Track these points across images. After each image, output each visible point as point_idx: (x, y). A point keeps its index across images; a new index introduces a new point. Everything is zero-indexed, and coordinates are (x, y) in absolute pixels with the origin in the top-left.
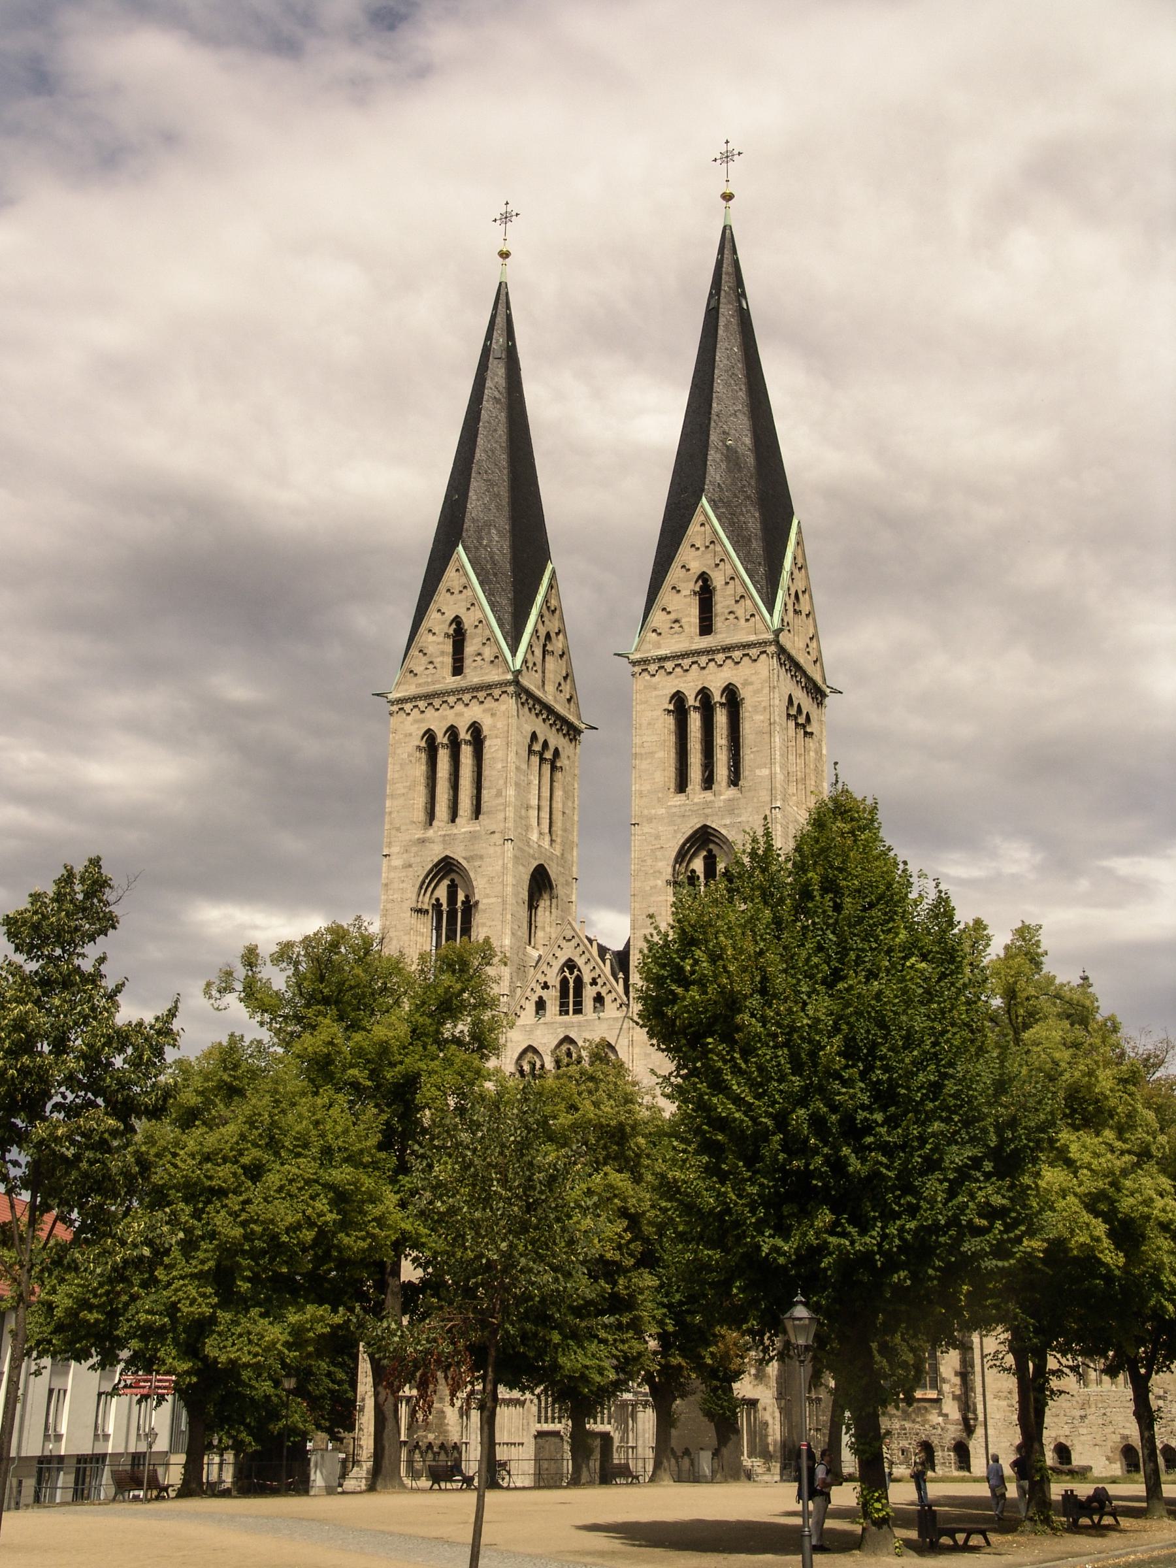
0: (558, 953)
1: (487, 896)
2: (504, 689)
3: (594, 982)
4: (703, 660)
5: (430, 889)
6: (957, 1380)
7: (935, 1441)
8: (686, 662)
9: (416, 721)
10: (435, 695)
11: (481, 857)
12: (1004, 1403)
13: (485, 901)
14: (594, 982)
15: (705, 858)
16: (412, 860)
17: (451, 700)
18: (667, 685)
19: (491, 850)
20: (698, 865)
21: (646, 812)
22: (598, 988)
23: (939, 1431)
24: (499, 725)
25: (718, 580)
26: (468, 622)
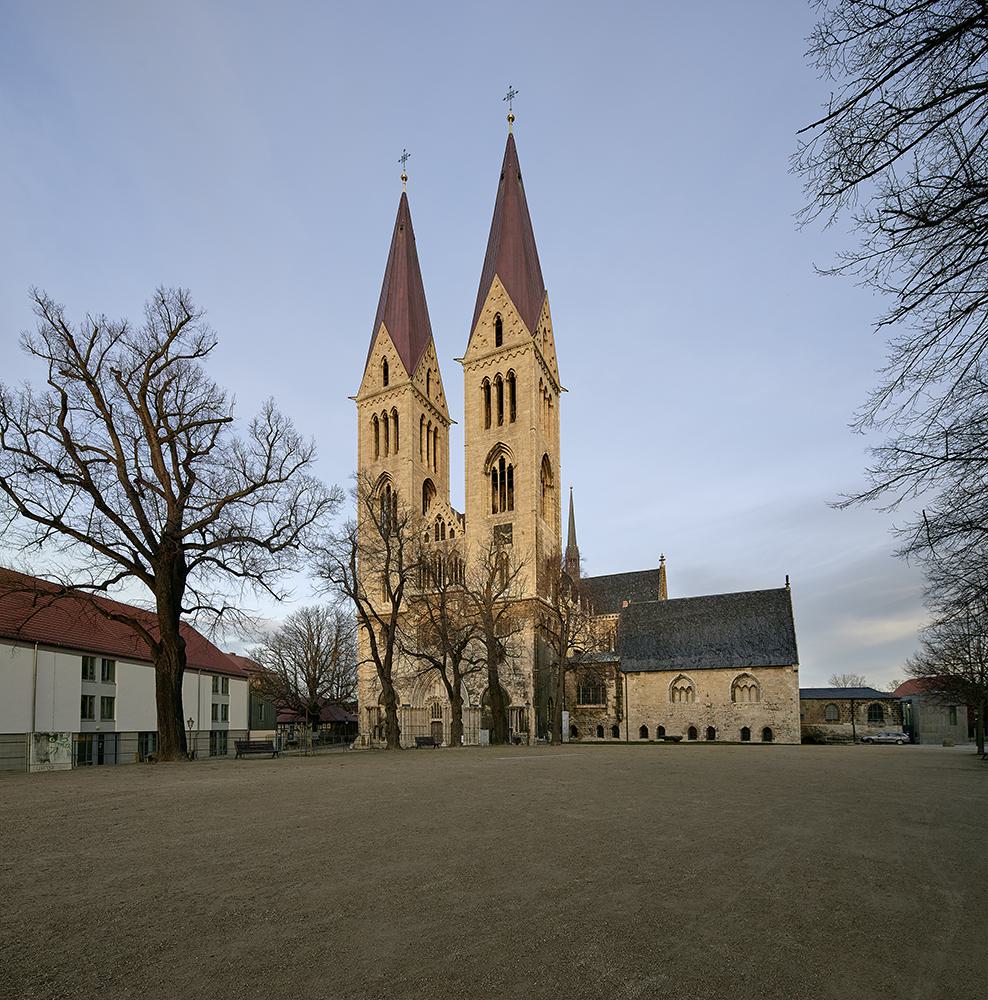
4: (498, 358)
8: (489, 360)
10: (376, 395)
17: (383, 397)
18: (481, 374)
20: (496, 465)
24: (405, 406)
25: (504, 316)
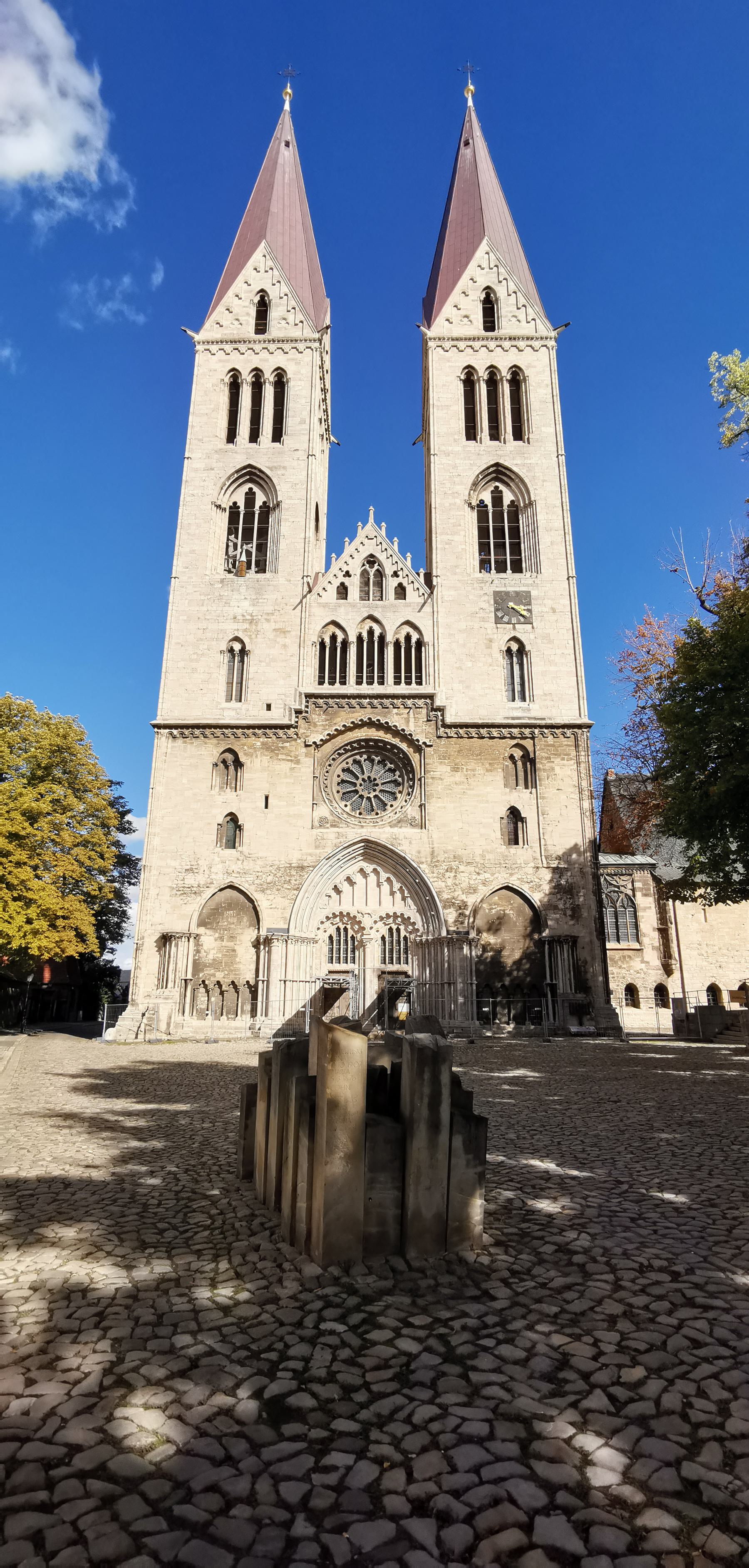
0: (361, 548)
1: (291, 498)
2: (309, 345)
3: (396, 574)
5: (232, 488)
6: (656, 935)
7: (639, 984)
9: (220, 361)
11: (285, 468)
12: (695, 953)
13: (288, 501)
14: (396, 574)
15: (492, 492)
16: (214, 465)
19: (295, 463)
20: (487, 497)
21: (443, 448)
22: (400, 580)
23: (643, 975)
24: (303, 371)
26: (273, 294)
